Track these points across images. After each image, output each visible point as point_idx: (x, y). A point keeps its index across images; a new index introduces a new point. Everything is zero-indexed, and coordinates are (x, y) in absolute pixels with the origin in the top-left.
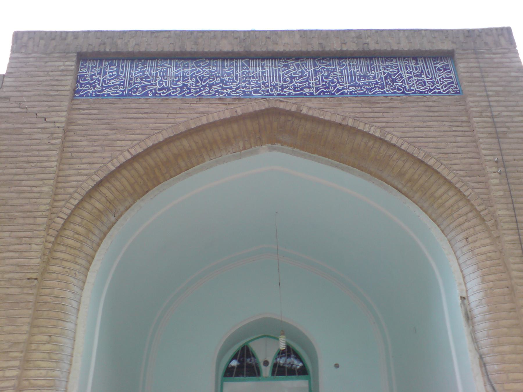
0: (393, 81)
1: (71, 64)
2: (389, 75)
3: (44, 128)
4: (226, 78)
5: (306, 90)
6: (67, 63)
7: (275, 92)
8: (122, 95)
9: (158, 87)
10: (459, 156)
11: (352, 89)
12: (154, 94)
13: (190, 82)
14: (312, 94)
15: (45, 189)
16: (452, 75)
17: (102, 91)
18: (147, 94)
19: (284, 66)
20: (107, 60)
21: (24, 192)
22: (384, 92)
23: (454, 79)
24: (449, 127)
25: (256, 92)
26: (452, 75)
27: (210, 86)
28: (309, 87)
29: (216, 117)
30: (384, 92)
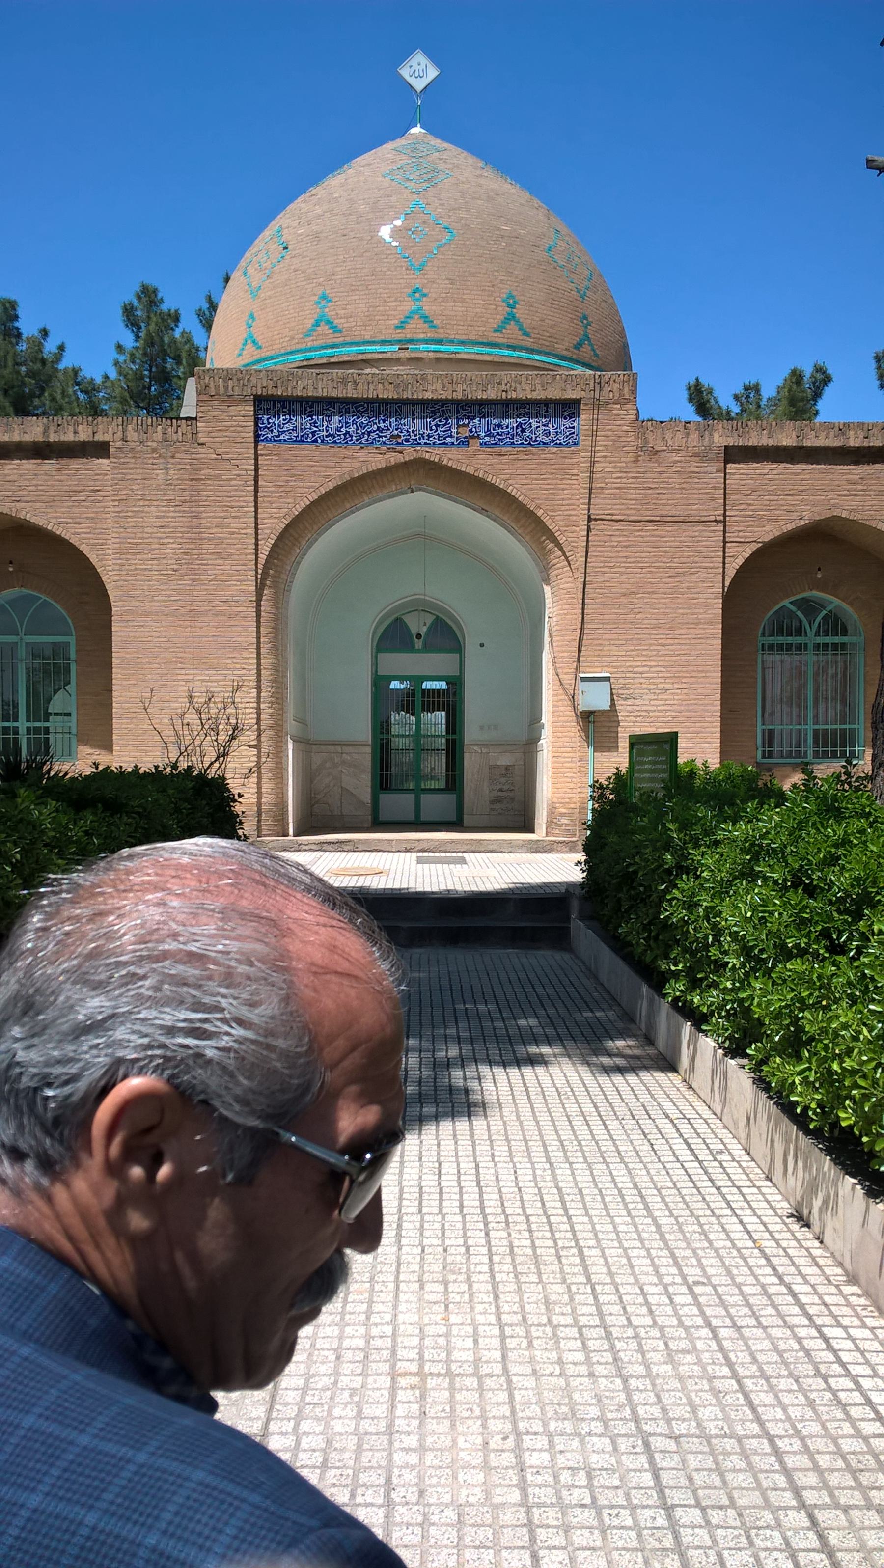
0: (523, 431)
1: (250, 409)
2: (520, 425)
3: (239, 475)
4: (382, 425)
5: (449, 440)
6: (247, 408)
7: (423, 442)
8: (296, 441)
9: (325, 433)
10: (563, 508)
11: (487, 439)
12: (322, 441)
13: (352, 429)
14: (453, 444)
15: (249, 531)
16: (575, 424)
17: (279, 436)
18: (316, 441)
19: (432, 412)
20: (279, 402)
21: (233, 533)
22: (513, 443)
23: (575, 430)
24: (561, 480)
25: (407, 440)
26: (575, 424)
27: (369, 433)
28: (451, 436)
29: (373, 467)
30: (513, 443)
